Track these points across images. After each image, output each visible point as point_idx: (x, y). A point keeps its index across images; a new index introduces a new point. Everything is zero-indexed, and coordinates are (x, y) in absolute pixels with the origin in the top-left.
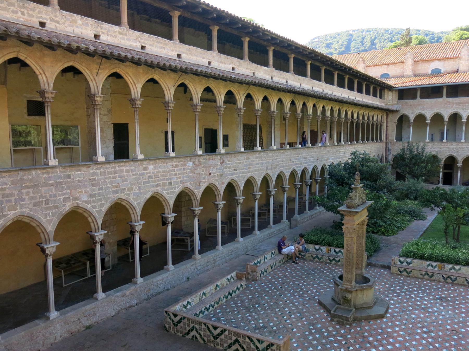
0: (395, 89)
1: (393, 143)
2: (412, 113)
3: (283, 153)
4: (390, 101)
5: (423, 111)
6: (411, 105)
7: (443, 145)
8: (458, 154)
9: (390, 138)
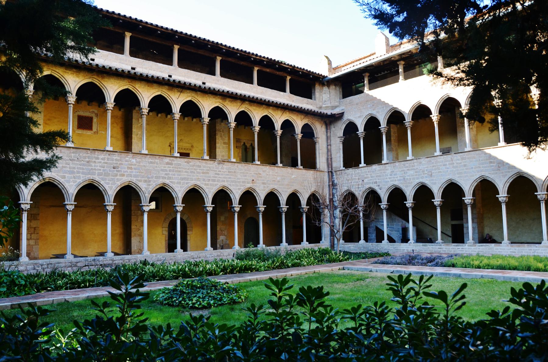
0: (326, 79)
1: (338, 173)
2: (360, 117)
4: (325, 101)
5: (374, 110)
6: (357, 104)
7: (407, 167)
8: (433, 180)
9: (334, 165)
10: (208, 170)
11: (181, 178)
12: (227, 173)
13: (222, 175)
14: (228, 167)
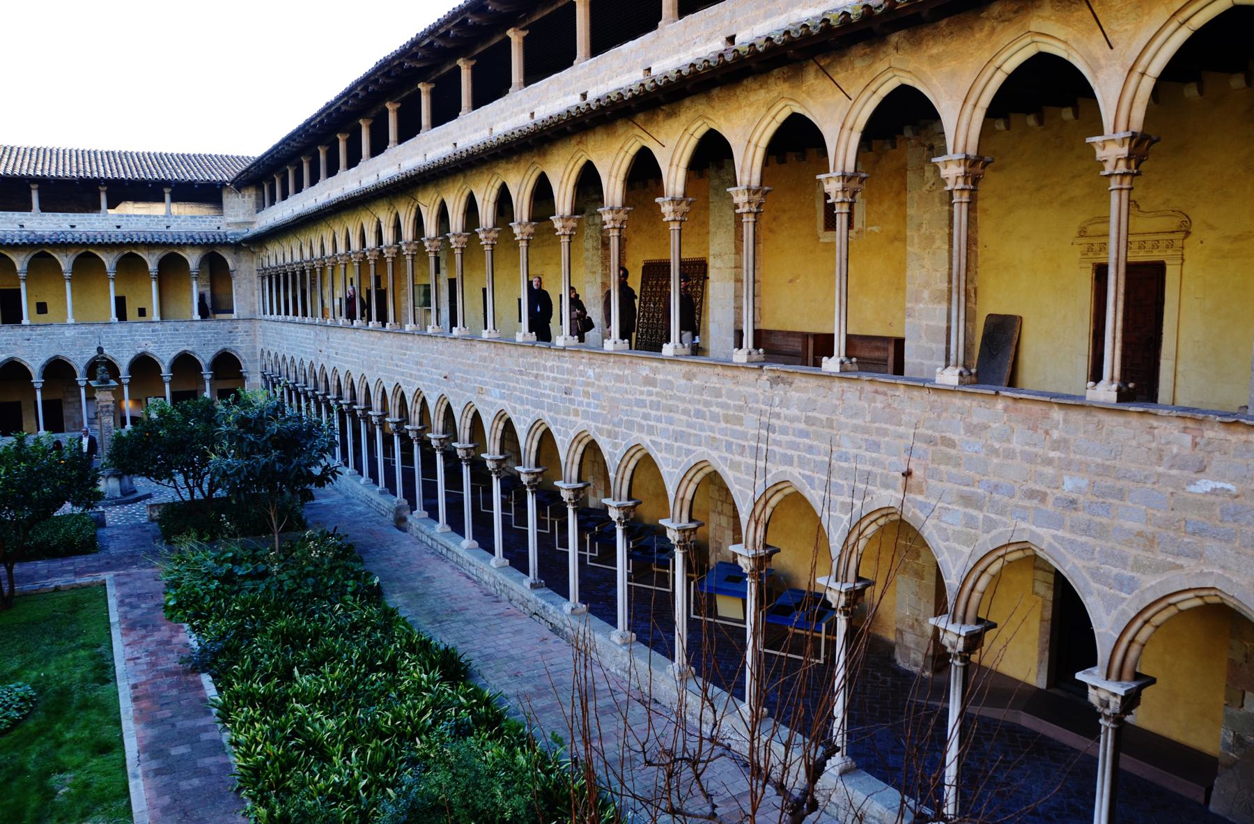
3: (380, 338)
10: (740, 408)
11: (673, 430)
12: (803, 426)
13: (784, 431)
14: (804, 396)
